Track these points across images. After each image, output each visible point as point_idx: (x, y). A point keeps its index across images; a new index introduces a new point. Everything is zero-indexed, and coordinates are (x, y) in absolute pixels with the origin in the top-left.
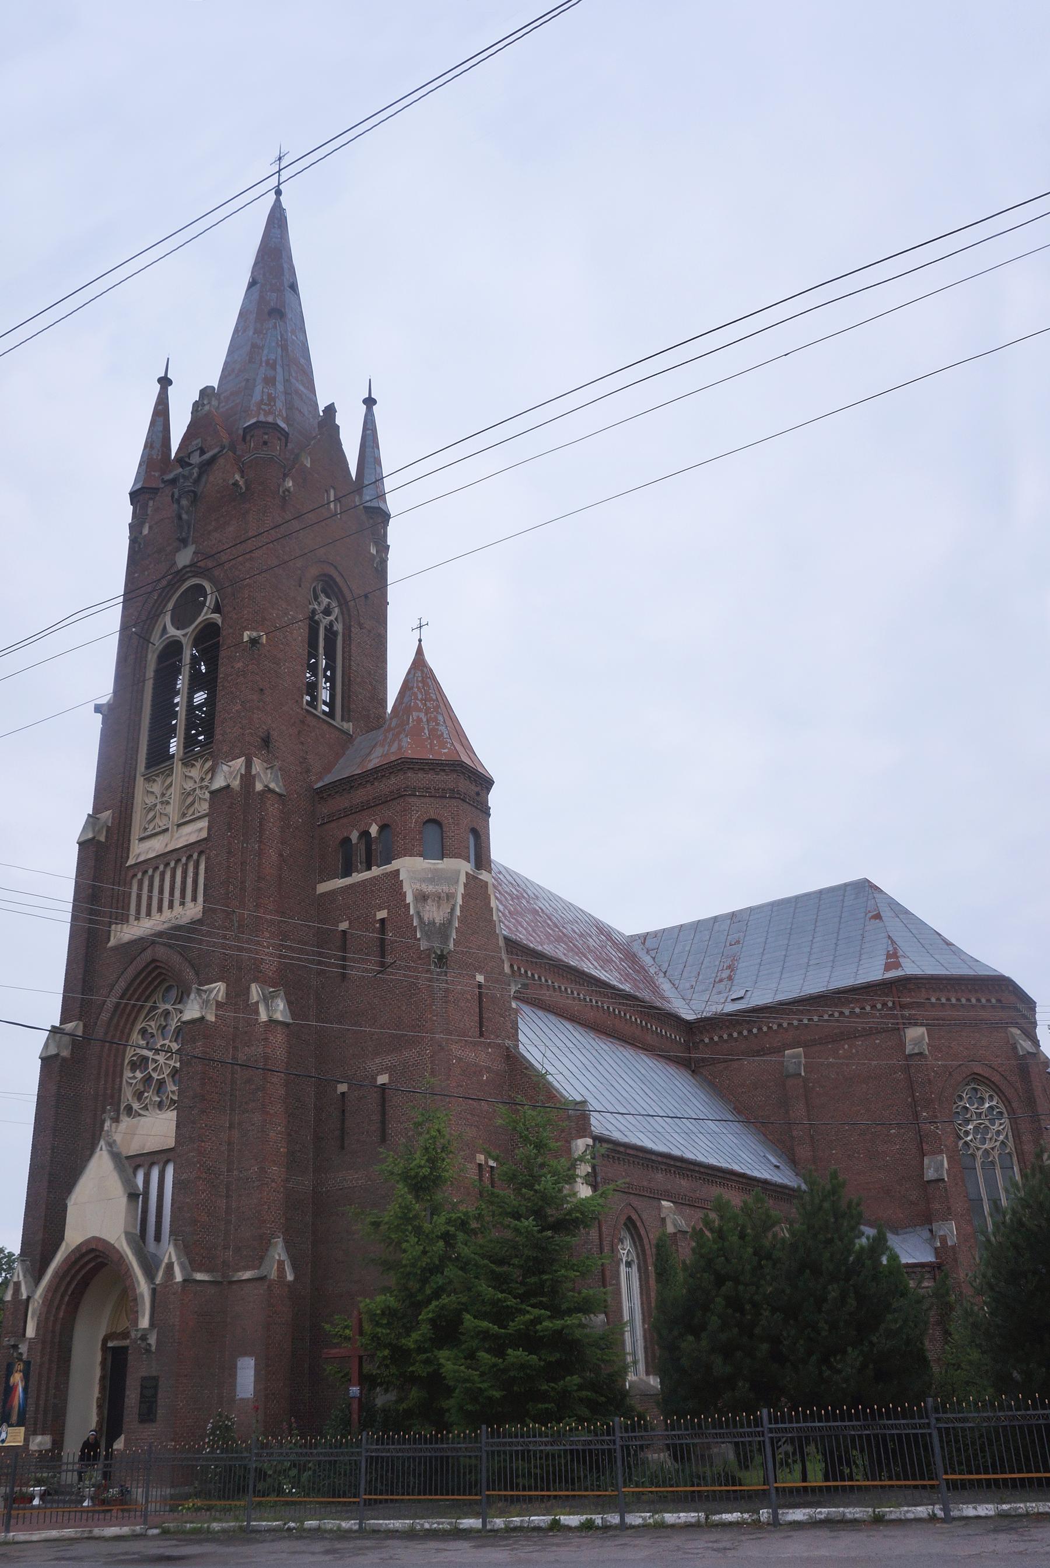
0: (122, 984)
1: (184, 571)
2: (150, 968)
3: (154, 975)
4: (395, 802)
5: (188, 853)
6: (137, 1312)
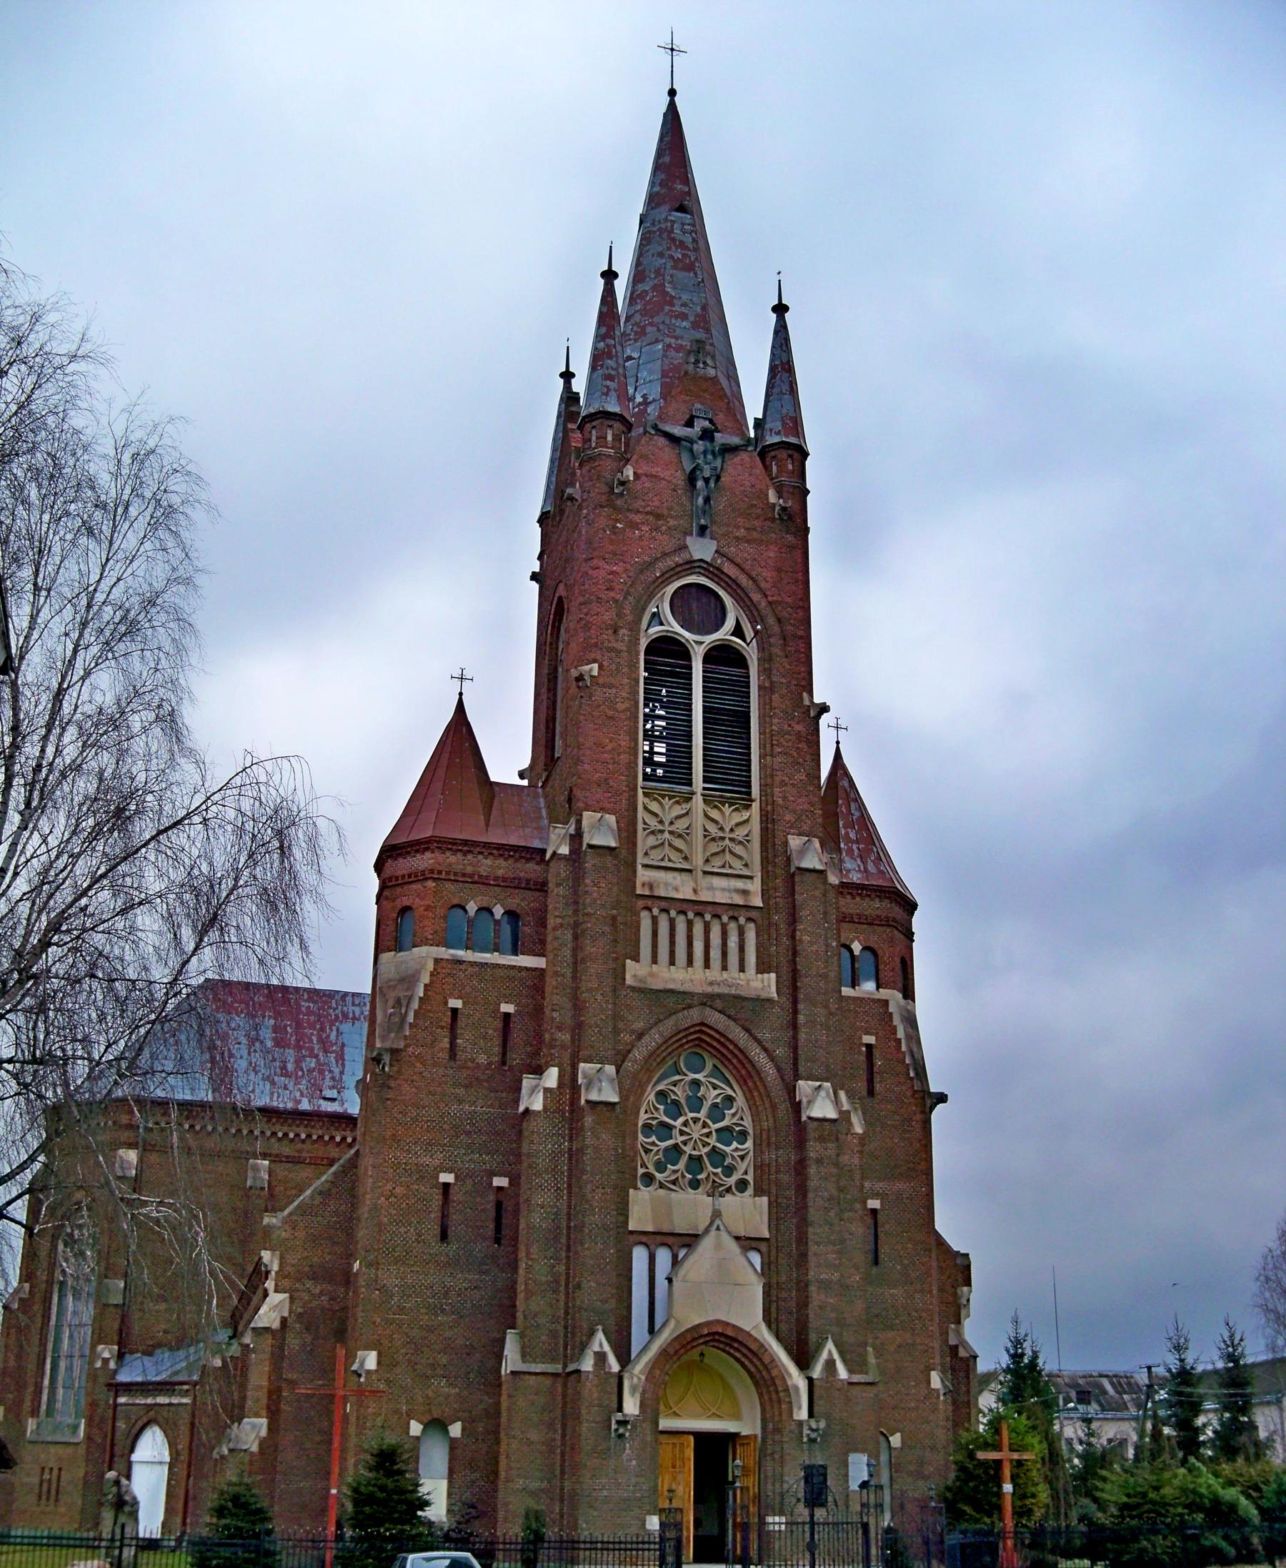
0: (653, 1040)
1: (696, 564)
2: (692, 1030)
3: (690, 1038)
4: (881, 929)
5: (731, 913)
6: (790, 1403)
